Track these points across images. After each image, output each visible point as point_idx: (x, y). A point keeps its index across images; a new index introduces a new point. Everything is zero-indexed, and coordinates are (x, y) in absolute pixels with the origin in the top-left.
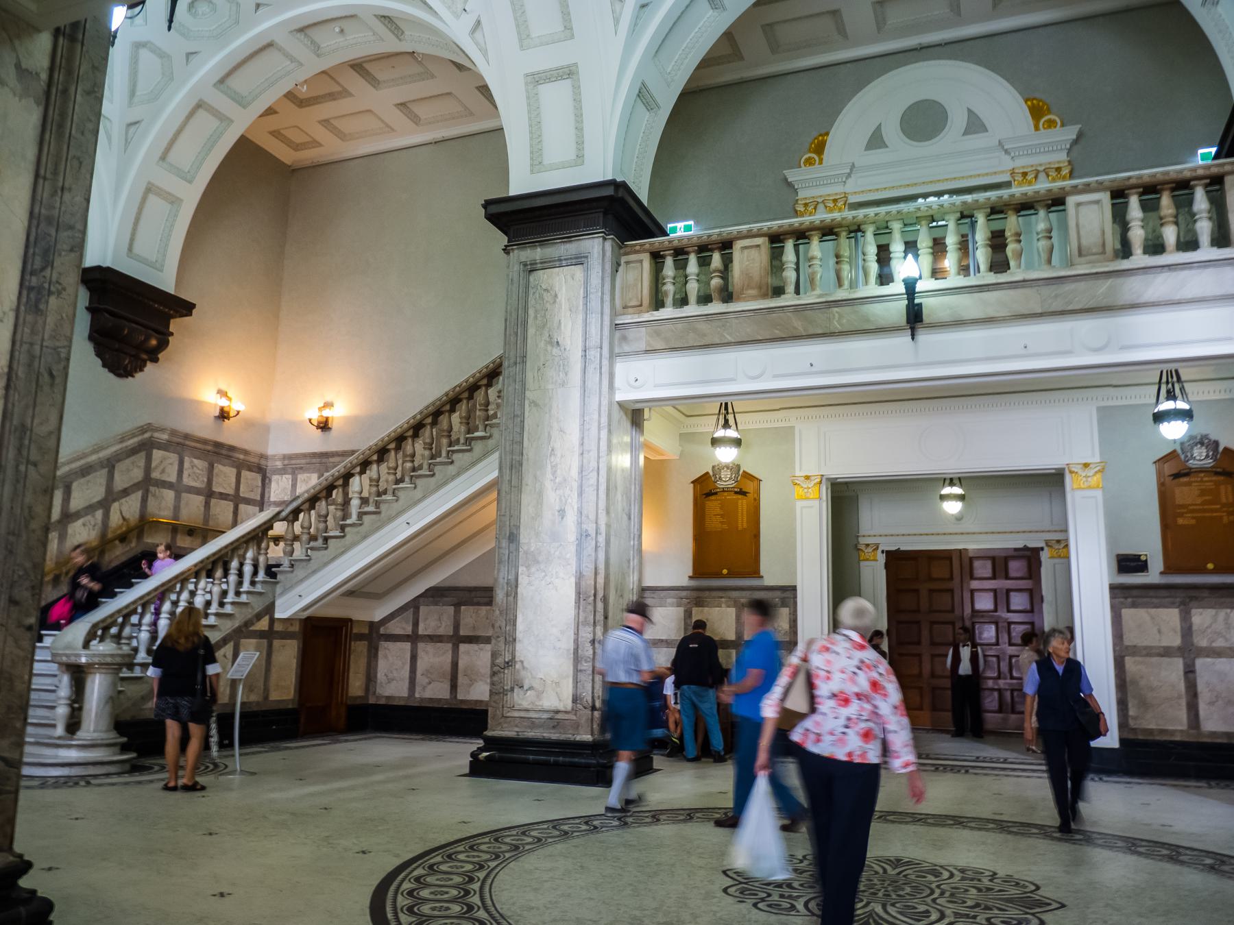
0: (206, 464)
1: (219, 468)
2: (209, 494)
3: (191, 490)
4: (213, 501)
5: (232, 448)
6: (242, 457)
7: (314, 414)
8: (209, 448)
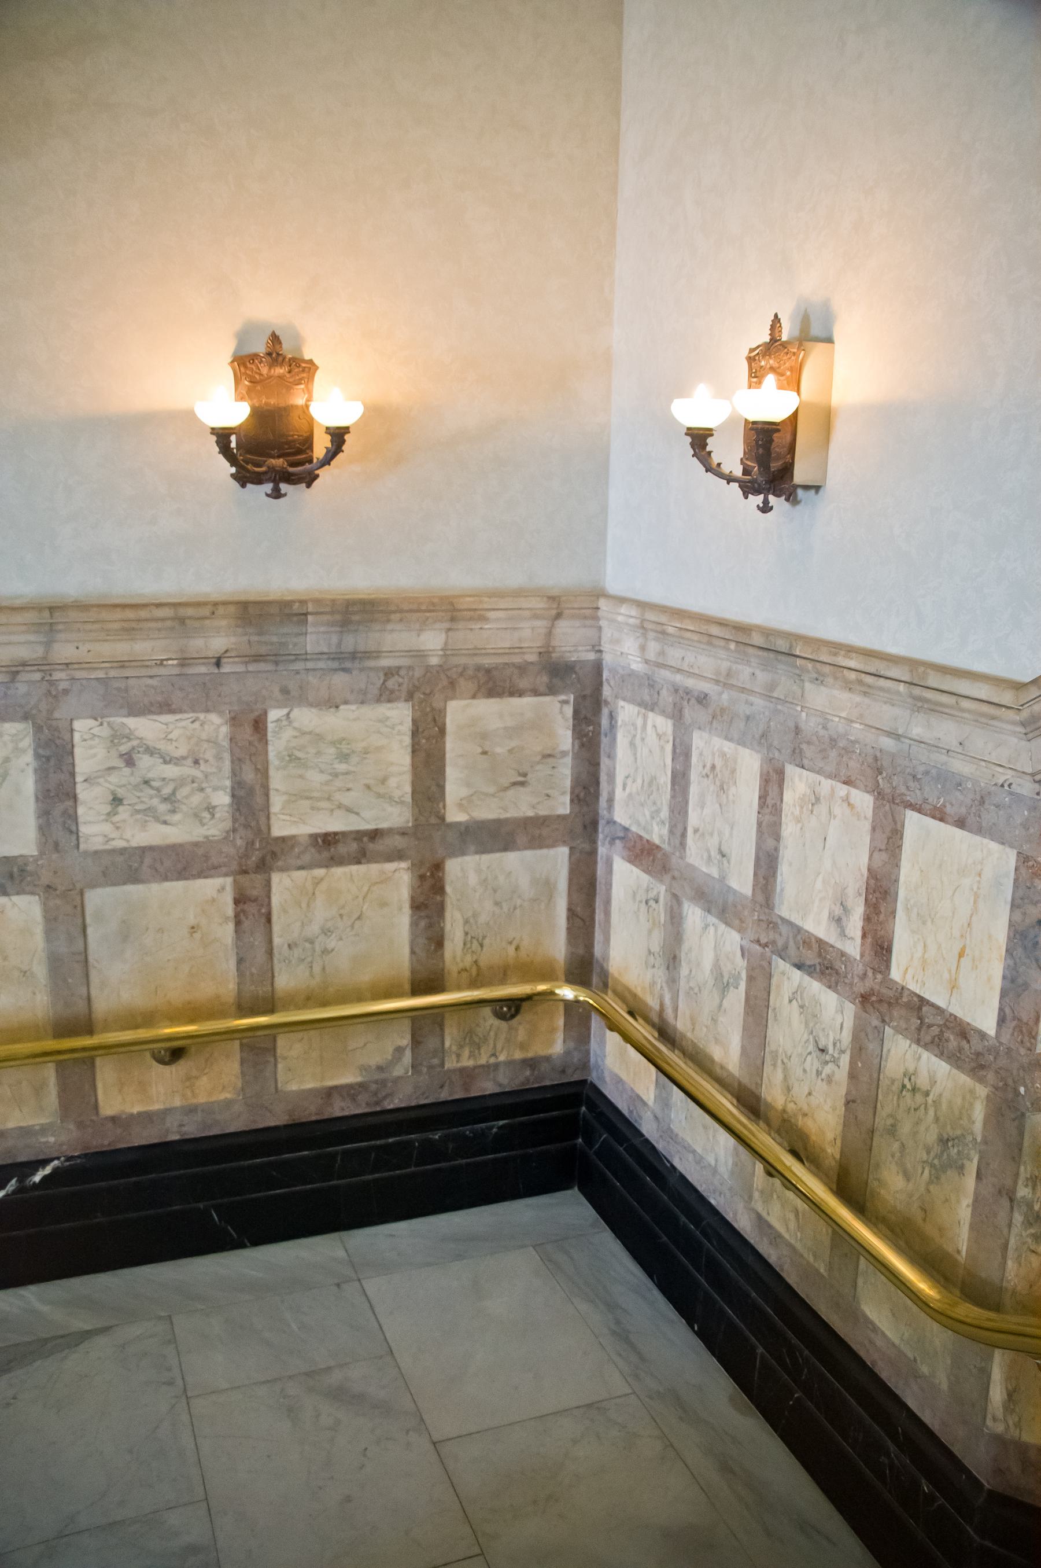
0: (216, 725)
1: (289, 726)
2: (255, 857)
3: (133, 866)
4: (283, 886)
5: (358, 612)
6: (432, 641)
7: (733, 402)
8: (218, 643)
